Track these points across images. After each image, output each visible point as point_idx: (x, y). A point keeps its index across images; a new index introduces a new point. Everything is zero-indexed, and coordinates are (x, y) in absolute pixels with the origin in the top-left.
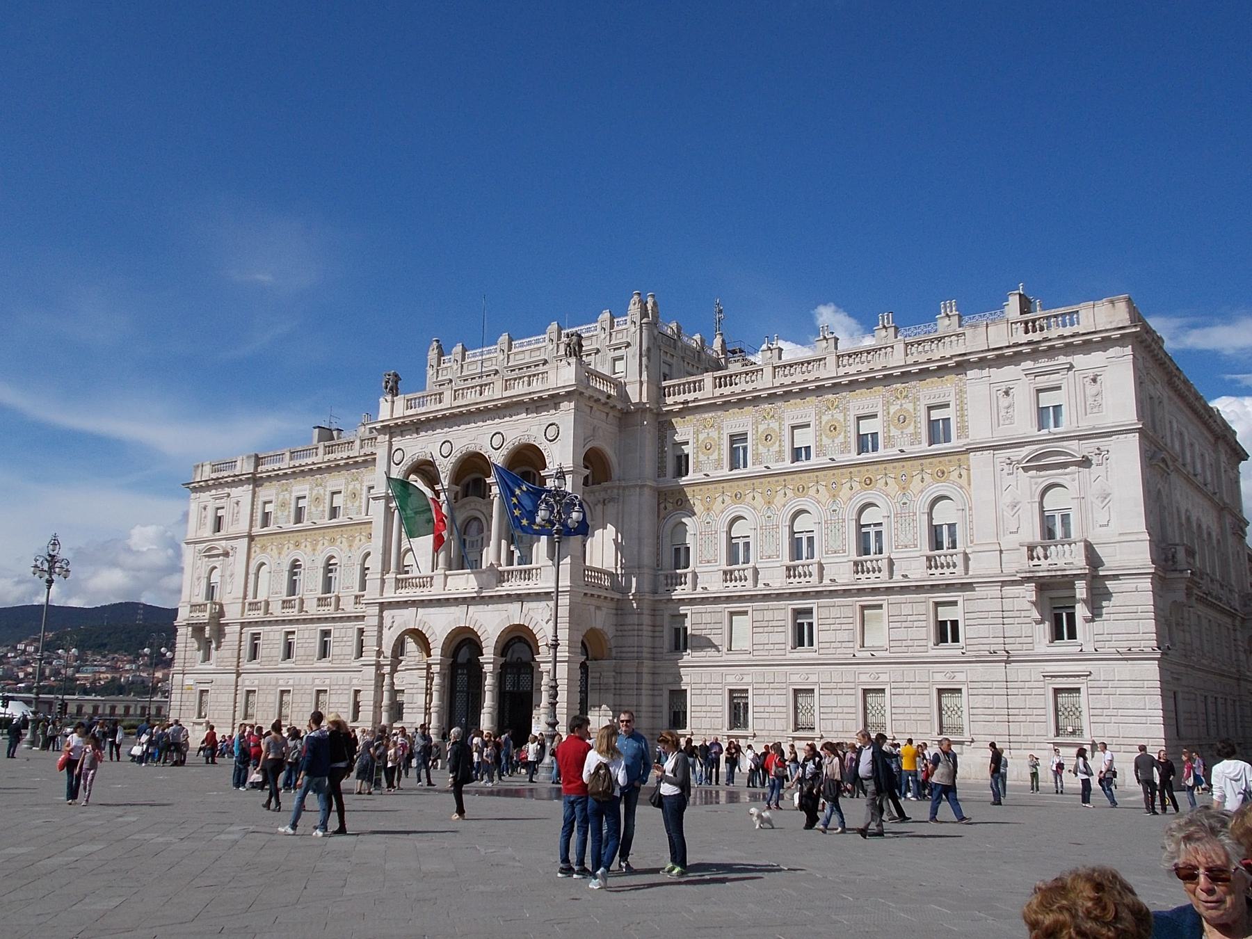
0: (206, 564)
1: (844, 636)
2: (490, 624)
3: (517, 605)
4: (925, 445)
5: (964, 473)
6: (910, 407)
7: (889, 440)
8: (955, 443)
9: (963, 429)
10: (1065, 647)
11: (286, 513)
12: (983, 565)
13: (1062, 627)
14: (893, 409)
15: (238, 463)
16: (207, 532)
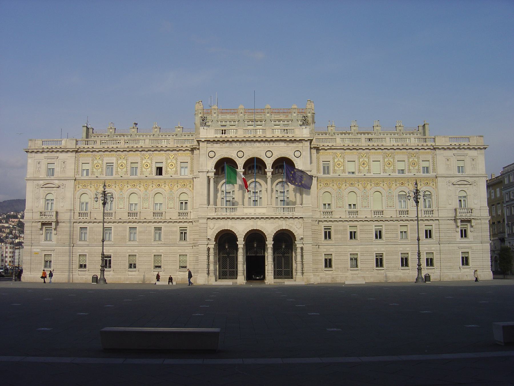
0: (42, 192)
1: (394, 235)
2: (269, 230)
3: (284, 222)
4: (422, 173)
5: (434, 184)
6: (416, 160)
7: (409, 171)
8: (432, 174)
9: (434, 170)
10: (464, 240)
11: (100, 170)
12: (443, 214)
13: (464, 234)
14: (410, 160)
15: (63, 142)
16: (43, 175)
